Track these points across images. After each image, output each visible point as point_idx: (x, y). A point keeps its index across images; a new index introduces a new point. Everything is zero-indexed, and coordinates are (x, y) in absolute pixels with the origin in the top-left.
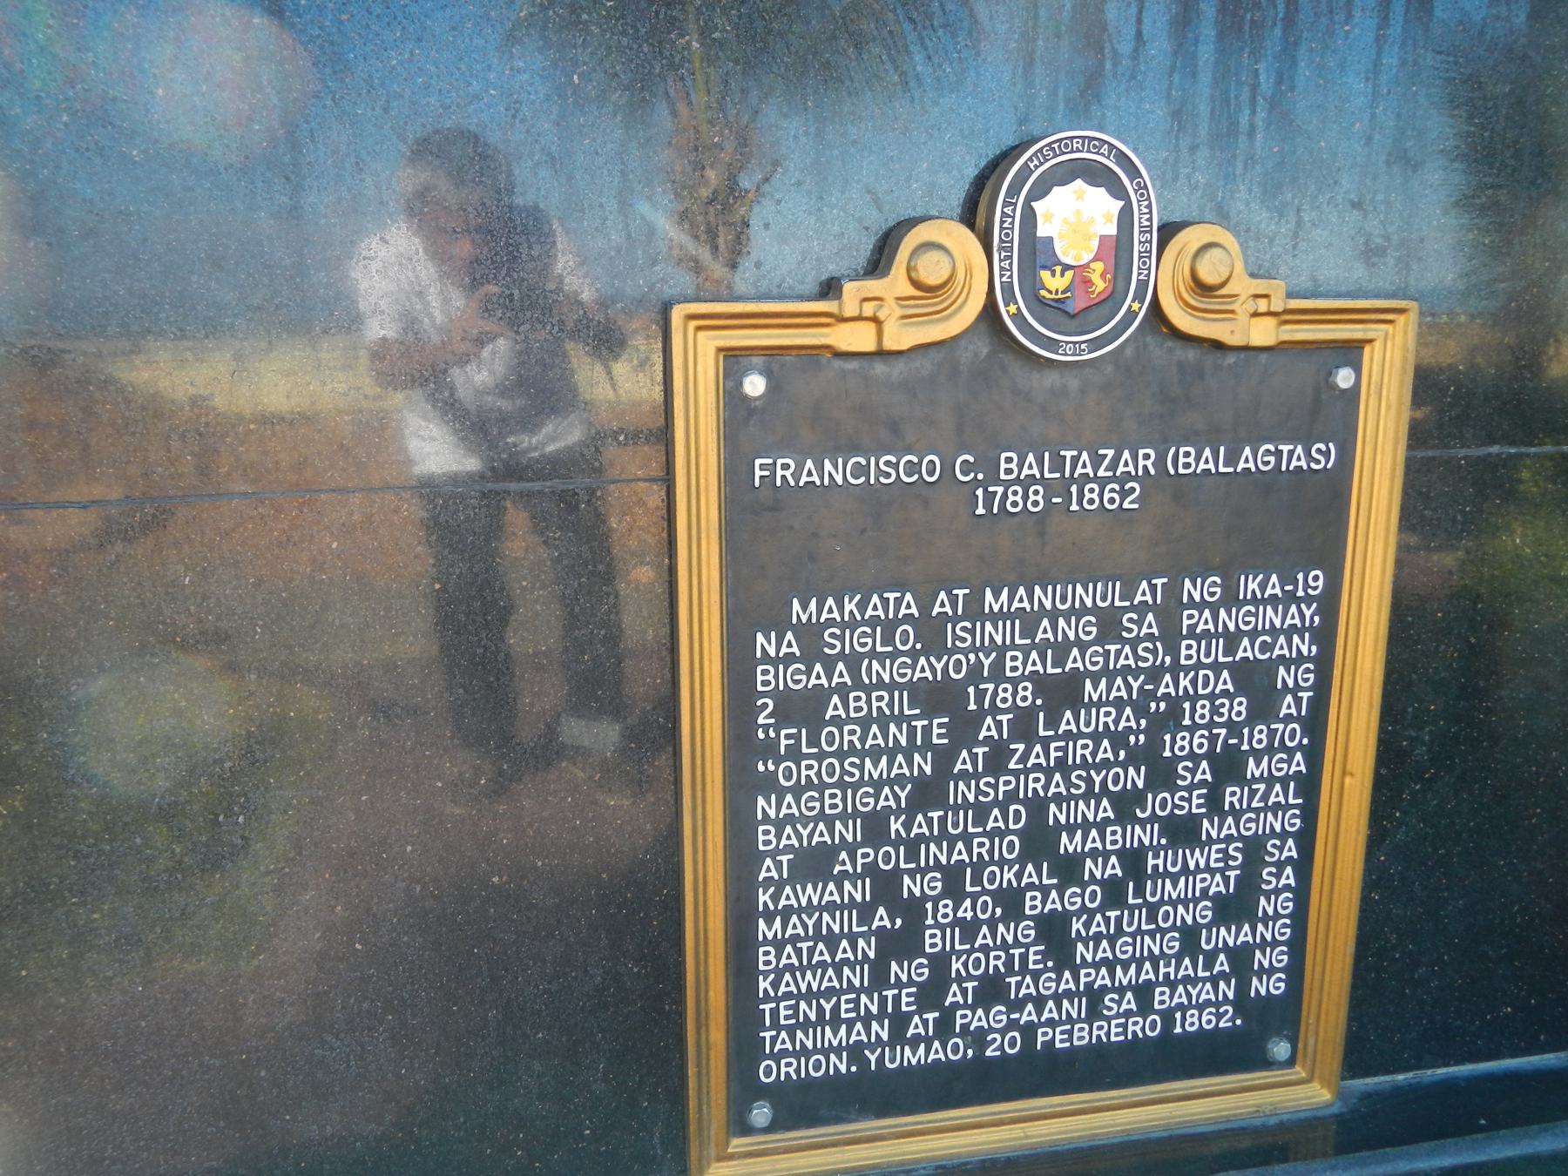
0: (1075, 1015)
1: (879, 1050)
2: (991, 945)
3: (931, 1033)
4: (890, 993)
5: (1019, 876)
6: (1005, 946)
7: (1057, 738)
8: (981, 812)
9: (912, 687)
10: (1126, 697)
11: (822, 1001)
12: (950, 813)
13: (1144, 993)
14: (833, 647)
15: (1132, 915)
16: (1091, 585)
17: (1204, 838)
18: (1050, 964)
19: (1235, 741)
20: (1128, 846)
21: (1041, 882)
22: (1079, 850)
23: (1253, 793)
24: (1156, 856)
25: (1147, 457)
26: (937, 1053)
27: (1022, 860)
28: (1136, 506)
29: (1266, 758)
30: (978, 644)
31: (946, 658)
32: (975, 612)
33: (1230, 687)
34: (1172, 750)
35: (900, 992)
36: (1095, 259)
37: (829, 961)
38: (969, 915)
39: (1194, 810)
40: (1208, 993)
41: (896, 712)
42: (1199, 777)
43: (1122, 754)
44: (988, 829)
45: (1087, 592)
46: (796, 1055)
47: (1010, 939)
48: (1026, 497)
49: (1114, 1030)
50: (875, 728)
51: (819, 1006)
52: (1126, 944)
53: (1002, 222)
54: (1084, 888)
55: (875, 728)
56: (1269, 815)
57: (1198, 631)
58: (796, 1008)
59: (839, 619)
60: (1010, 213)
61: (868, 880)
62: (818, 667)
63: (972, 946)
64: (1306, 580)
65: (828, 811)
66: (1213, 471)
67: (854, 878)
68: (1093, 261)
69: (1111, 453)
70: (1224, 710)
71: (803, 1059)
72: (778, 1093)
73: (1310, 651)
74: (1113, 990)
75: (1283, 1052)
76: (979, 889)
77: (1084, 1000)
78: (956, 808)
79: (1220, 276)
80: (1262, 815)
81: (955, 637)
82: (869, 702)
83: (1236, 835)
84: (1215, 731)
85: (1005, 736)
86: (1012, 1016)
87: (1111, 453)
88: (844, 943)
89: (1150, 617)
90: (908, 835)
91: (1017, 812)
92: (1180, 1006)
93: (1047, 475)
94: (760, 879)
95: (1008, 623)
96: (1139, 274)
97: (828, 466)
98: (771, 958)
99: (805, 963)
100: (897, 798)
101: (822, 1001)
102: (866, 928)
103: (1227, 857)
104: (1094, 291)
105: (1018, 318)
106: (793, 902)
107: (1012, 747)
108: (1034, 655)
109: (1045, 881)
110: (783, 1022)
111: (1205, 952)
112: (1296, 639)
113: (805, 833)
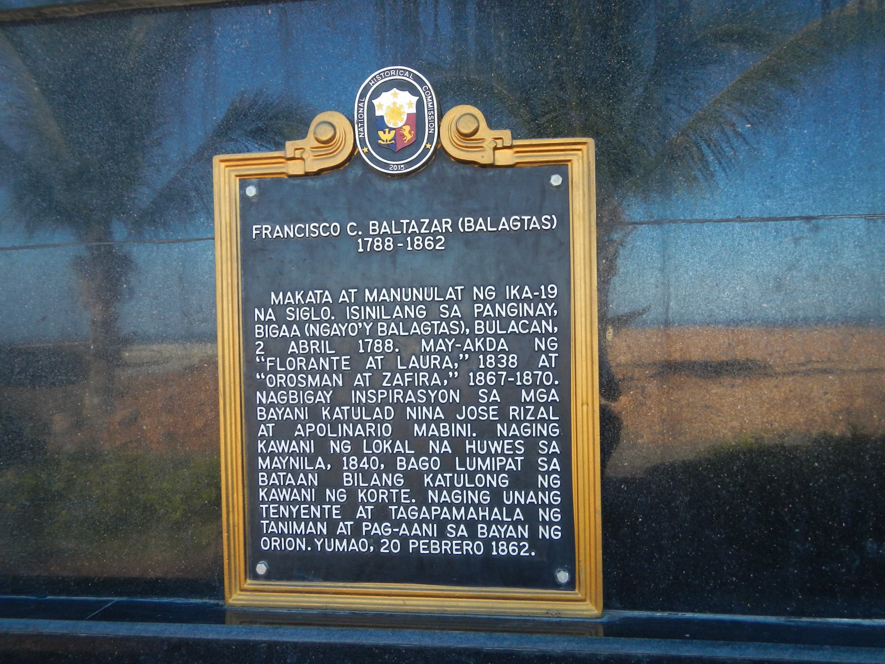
0: (430, 535)
1: (322, 539)
2: (380, 485)
3: (349, 534)
4: (327, 507)
5: (392, 446)
7: (407, 370)
10: (445, 350)
11: (291, 506)
13: (471, 526)
14: (291, 317)
18: (414, 501)
19: (513, 379)
20: (453, 435)
23: (526, 411)
25: (447, 223)
26: (354, 546)
27: (394, 438)
29: (533, 390)
30: (363, 318)
31: (346, 324)
32: (361, 302)
33: (505, 347)
34: (474, 381)
35: (332, 507)
36: (406, 124)
37: (294, 484)
38: (366, 466)
39: (491, 418)
40: (511, 532)
41: (323, 352)
43: (446, 382)
45: (419, 292)
47: (390, 483)
48: (383, 243)
49: (455, 547)
50: (313, 360)
53: (358, 110)
54: (430, 457)
55: (313, 360)
59: (293, 303)
62: (284, 327)
63: (369, 485)
64: (546, 289)
66: (485, 230)
68: (404, 125)
69: (427, 221)
70: (504, 361)
71: (283, 539)
72: (269, 556)
73: (553, 330)
74: (452, 521)
76: (371, 452)
77: (435, 525)
80: (534, 425)
82: (309, 345)
83: (519, 435)
84: (499, 373)
86: (394, 530)
88: (302, 475)
89: (456, 307)
90: (332, 418)
93: (394, 232)
94: (259, 435)
95: (378, 307)
96: (429, 130)
99: (282, 484)
100: (325, 398)
101: (291, 506)
102: (312, 468)
103: (514, 448)
104: (405, 140)
105: (368, 154)
106: (275, 449)
107: (384, 374)
109: (407, 452)
110: (272, 516)
112: (544, 322)
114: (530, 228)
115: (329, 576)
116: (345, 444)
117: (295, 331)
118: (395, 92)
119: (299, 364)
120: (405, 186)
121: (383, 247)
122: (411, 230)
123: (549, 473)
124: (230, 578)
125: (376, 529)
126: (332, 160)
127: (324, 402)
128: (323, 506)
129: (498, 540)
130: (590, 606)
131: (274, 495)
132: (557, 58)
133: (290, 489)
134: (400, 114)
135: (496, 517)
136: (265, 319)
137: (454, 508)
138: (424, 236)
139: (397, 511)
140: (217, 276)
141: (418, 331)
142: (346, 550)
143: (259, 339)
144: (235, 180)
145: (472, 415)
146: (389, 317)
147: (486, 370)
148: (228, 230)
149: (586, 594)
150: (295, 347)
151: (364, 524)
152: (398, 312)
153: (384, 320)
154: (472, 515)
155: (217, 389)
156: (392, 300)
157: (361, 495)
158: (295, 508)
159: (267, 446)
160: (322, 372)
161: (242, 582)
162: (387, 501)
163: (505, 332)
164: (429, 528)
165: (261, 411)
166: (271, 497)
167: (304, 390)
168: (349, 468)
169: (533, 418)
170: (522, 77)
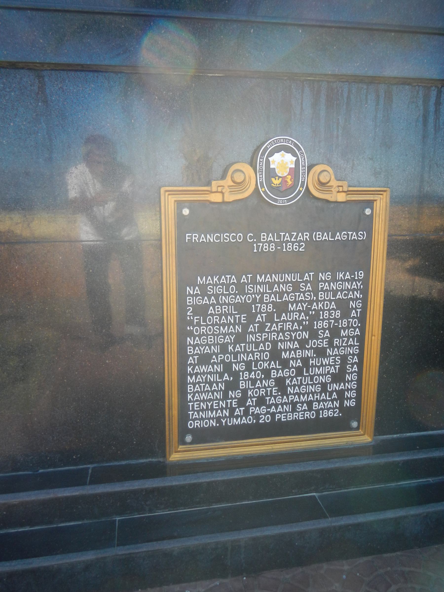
0: (288, 410)
1: (226, 419)
2: (261, 387)
3: (242, 414)
4: (229, 401)
5: (269, 365)
8: (257, 345)
9: (234, 304)
10: (302, 309)
11: (208, 403)
12: (247, 344)
13: (310, 404)
14: (210, 292)
16: (290, 274)
17: (328, 355)
18: (279, 393)
19: (337, 324)
20: (304, 356)
21: (276, 367)
22: (288, 357)
23: (343, 341)
24: (312, 360)
25: (306, 235)
26: (244, 421)
27: (270, 360)
28: (304, 250)
29: (347, 330)
30: (255, 292)
31: (245, 296)
32: (254, 282)
33: (335, 307)
34: (317, 326)
35: (232, 401)
36: (288, 175)
37: (210, 390)
38: (254, 377)
39: (324, 346)
41: (230, 312)
42: (325, 335)
43: (301, 327)
44: (259, 350)
45: (289, 276)
46: (200, 420)
47: (267, 385)
48: (269, 247)
49: (300, 416)
50: (223, 317)
51: (207, 404)
52: (303, 388)
53: (260, 163)
54: (290, 369)
55: (223, 317)
56: (349, 348)
57: (324, 289)
58: (200, 404)
59: (212, 283)
60: (262, 161)
61: (222, 365)
62: (206, 298)
63: (255, 387)
65: (209, 343)
66: (328, 240)
67: (217, 364)
68: (287, 175)
69: (295, 234)
70: (333, 314)
71: (202, 421)
72: (194, 432)
74: (300, 403)
75: (355, 425)
76: (257, 369)
77: (291, 405)
78: (249, 343)
79: (326, 180)
80: (346, 348)
81: (248, 289)
82: (222, 309)
83: (338, 354)
84: (330, 321)
85: (264, 321)
86: (268, 410)
87: (295, 234)
88: (215, 384)
89: (309, 285)
90: (234, 351)
91: (268, 345)
92: (321, 409)
93: (276, 240)
95: (265, 285)
96: (302, 179)
98: (192, 388)
99: (202, 390)
100: (231, 339)
101: (208, 403)
102: (221, 380)
103: (335, 361)
105: (265, 192)
106: (199, 371)
107: (266, 324)
108: (273, 295)
109: (278, 367)
110: (195, 409)
111: (329, 392)
112: (355, 292)
113: (202, 349)
114: (352, 239)
118: (283, 153)
121: (269, 249)
125: (257, 411)
128: (227, 401)
137: (301, 395)
138: (293, 243)
141: (287, 299)
142: (239, 423)
143: (189, 306)
145: (314, 344)
147: (323, 320)
152: (276, 288)
154: (311, 398)
157: (250, 393)
160: (229, 325)
163: (335, 298)
169: (346, 345)
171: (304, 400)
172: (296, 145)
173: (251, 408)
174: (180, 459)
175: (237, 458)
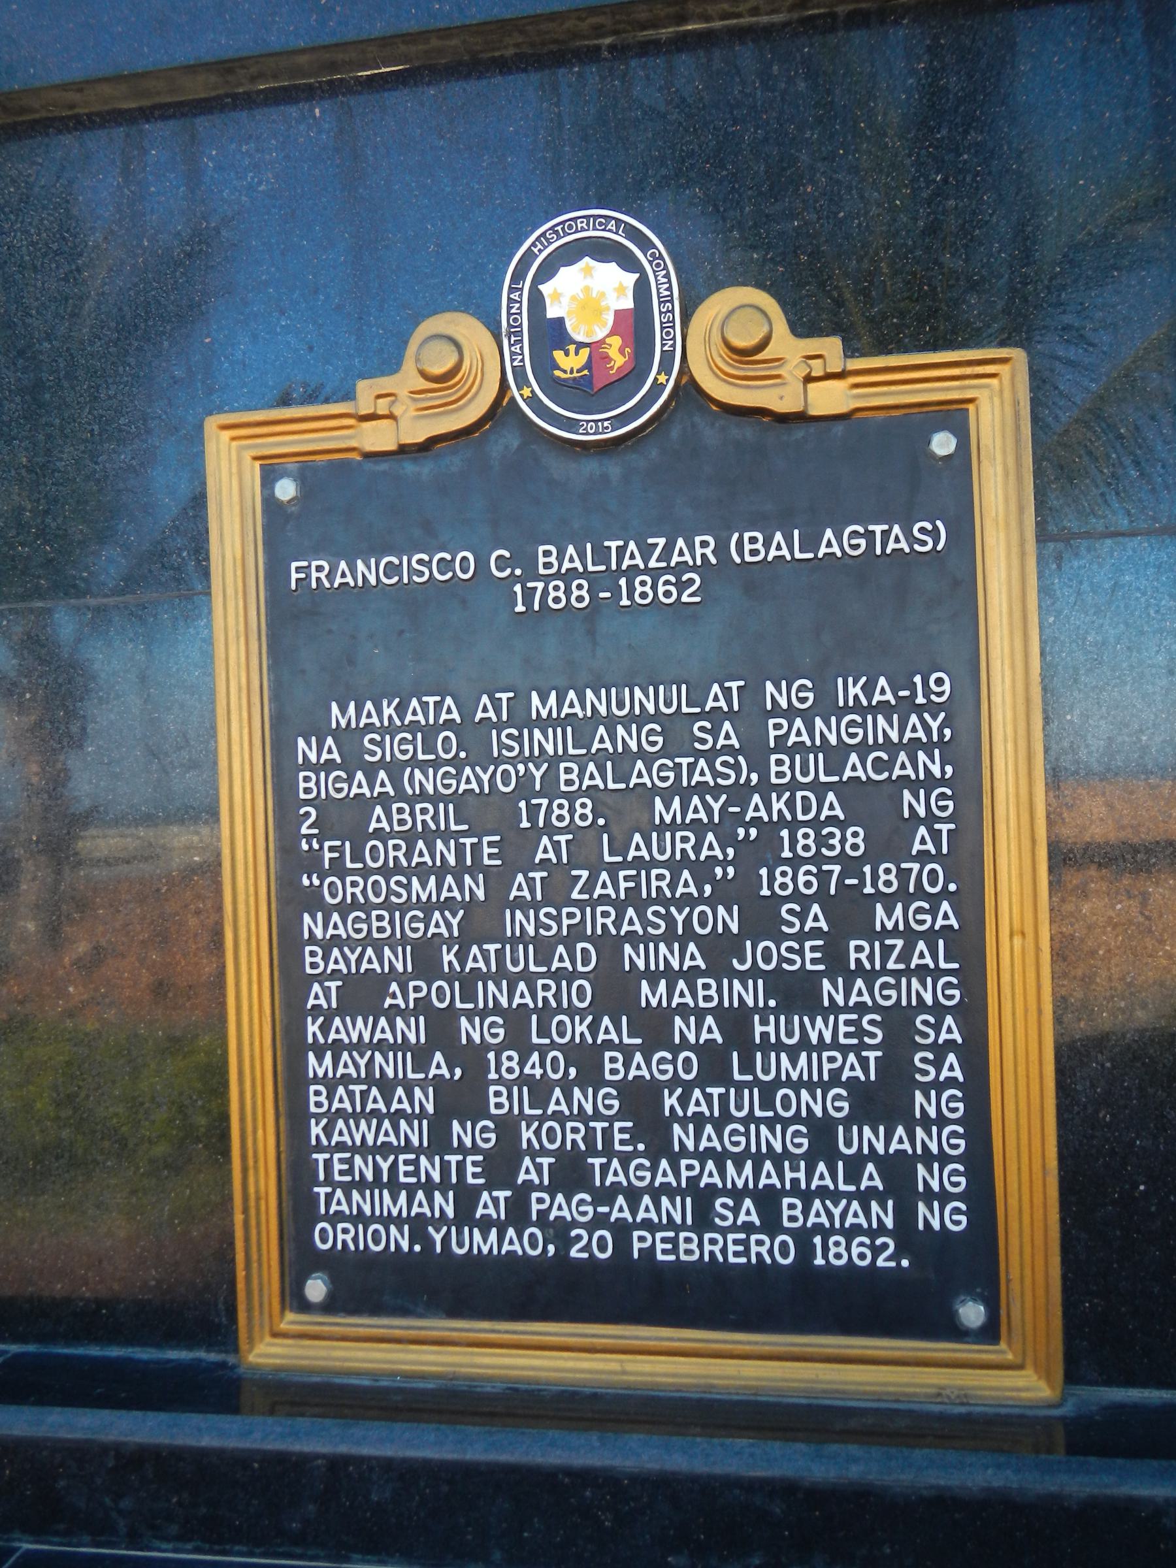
0: (678, 1220)
1: (445, 1229)
2: (567, 1113)
3: (503, 1217)
4: (454, 1159)
5: (594, 1028)
6: (582, 1116)
7: (624, 865)
8: (544, 954)
9: (459, 800)
10: (705, 820)
11: (378, 1158)
13: (768, 1201)
14: (373, 754)
15: (738, 1096)
16: (651, 689)
18: (641, 1147)
19: (855, 881)
20: (726, 1004)
23: (887, 951)
25: (704, 544)
26: (514, 1244)
27: (597, 1010)
28: (697, 599)
29: (899, 906)
30: (527, 754)
31: (492, 768)
32: (521, 719)
33: (838, 812)
35: (465, 1159)
36: (612, 333)
37: (384, 1110)
38: (538, 1072)
39: (809, 967)
40: (856, 1215)
41: (443, 827)
43: (708, 889)
45: (647, 697)
46: (351, 1219)
47: (589, 1109)
48: (568, 592)
49: (731, 1248)
50: (420, 844)
53: (509, 308)
54: (675, 1051)
55: (420, 844)
56: (914, 981)
59: (378, 724)
62: (360, 775)
63: (545, 1112)
64: (925, 683)
65: (376, 935)
66: (788, 558)
67: (404, 1013)
68: (608, 336)
69: (662, 541)
70: (835, 842)
71: (361, 1227)
73: (943, 772)
74: (724, 1192)
76: (547, 1041)
78: (514, 941)
80: (904, 981)
82: (412, 814)
83: (870, 1003)
84: (825, 868)
86: (601, 1209)
88: (400, 1091)
89: (727, 726)
92: (818, 1228)
93: (591, 568)
94: (309, 1006)
95: (559, 730)
96: (663, 345)
97: (360, 565)
99: (358, 1109)
100: (449, 926)
101: (378, 1158)
102: (422, 1076)
103: (861, 1033)
104: (612, 368)
105: (533, 401)
106: (343, 1036)
107: (574, 873)
109: (626, 1040)
110: (337, 1178)
111: (847, 1159)
112: (922, 756)
114: (888, 551)
115: (458, 1309)
116: (493, 1025)
117: (383, 785)
118: (587, 264)
119: (392, 854)
120: (613, 468)
121: (568, 600)
122: (626, 563)
123: (939, 1086)
124: (249, 1310)
125: (560, 1208)
126: (455, 416)
127: (446, 935)
128: (447, 1158)
129: (826, 1233)
130: (1035, 1378)
131: (341, 1134)
132: (934, 181)
133: (374, 1122)
134: (599, 312)
135: (822, 1183)
136: (318, 759)
139: (605, 1169)
140: (217, 671)
141: (646, 780)
142: (495, 1252)
143: (307, 802)
144: (253, 468)
145: (767, 959)
146: (584, 751)
147: (796, 862)
148: (239, 573)
149: (1024, 1353)
150: (383, 817)
151: (535, 1195)
153: (573, 758)
154: (769, 1177)
155: (220, 909)
156: (589, 714)
157: (527, 1134)
158: (385, 1160)
159: (325, 1029)
160: (442, 871)
161: (276, 1319)
162: (583, 1147)
163: (836, 779)
164: (674, 1206)
165: (313, 954)
166: (336, 1138)
167: (404, 908)
168: (501, 1076)
170: (860, 225)
171: (740, 1184)
172: (634, 234)
173: (535, 1195)
174: (284, 1361)
175: (479, 1390)
